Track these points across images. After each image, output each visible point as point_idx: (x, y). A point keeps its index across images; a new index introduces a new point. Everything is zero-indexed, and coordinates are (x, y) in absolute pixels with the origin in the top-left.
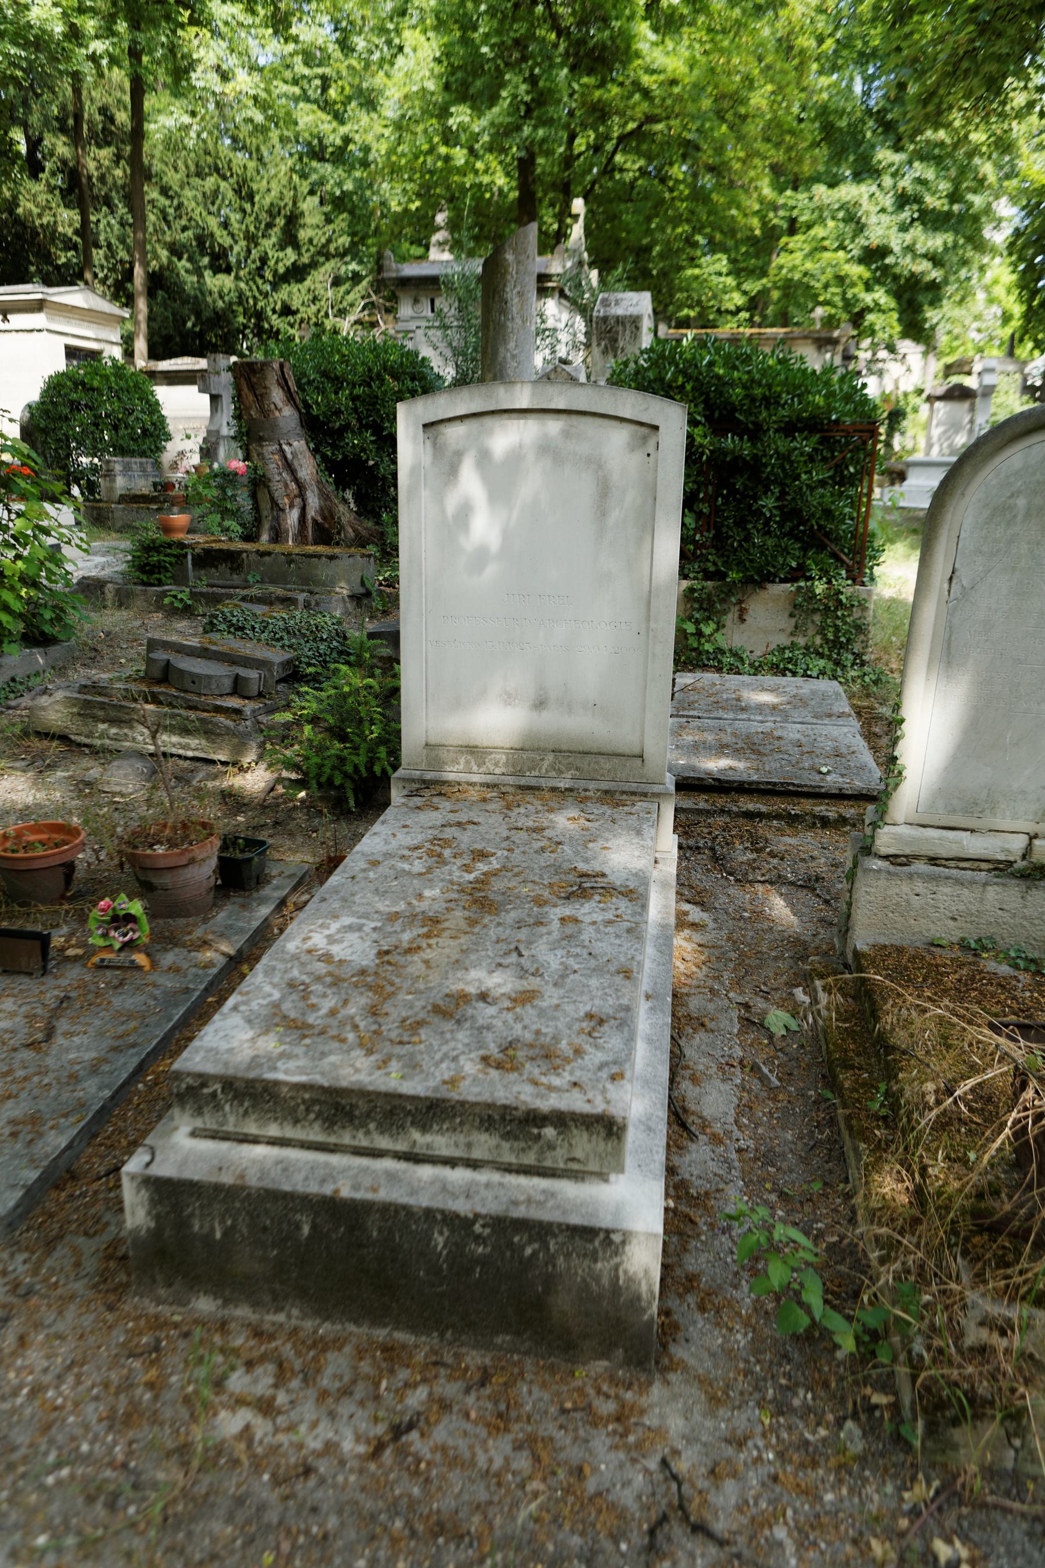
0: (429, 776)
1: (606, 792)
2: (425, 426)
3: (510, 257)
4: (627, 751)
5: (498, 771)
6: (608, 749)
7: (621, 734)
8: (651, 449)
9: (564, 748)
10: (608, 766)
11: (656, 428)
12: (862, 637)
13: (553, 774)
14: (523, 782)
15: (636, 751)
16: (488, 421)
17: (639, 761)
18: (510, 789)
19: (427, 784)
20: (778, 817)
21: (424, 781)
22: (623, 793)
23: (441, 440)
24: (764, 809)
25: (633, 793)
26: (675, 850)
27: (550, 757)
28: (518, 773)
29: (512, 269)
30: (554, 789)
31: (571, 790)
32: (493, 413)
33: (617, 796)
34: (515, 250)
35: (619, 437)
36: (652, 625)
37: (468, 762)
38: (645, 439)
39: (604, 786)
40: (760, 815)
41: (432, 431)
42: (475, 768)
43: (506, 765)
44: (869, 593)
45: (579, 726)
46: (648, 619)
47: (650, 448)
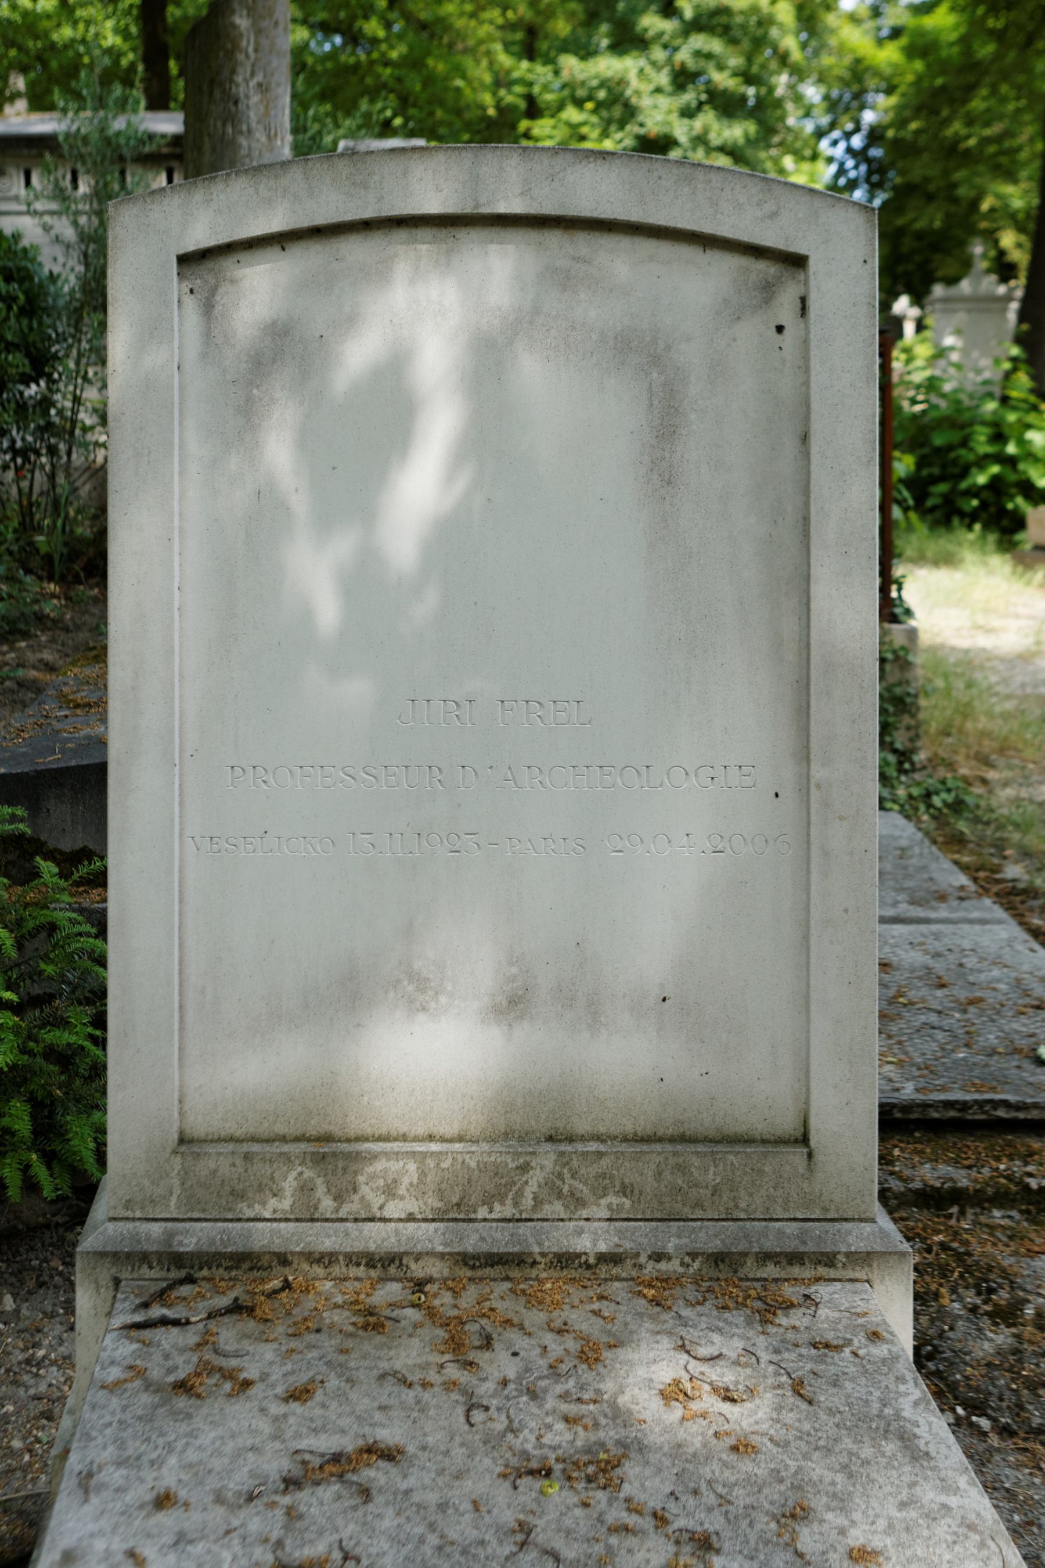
0: (193, 1238)
1: (718, 1259)
2: (185, 260)
3: (242, 21)
4: (759, 1127)
5: (394, 1209)
6: (705, 1122)
7: (753, 1089)
8: (785, 310)
9: (582, 1126)
10: (712, 1177)
11: (797, 262)
12: (907, 720)
13: (557, 1208)
14: (472, 1240)
15: (787, 1124)
16: (355, 250)
17: (796, 1157)
18: (435, 1269)
19: (185, 1268)
20: (1001, 1199)
21: (178, 1259)
22: (766, 1257)
23: (224, 296)
24: (963, 1179)
25: (795, 1258)
26: (951, 1436)
27: (546, 1159)
28: (455, 1212)
29: (247, 43)
30: (564, 1260)
31: (612, 1258)
32: (366, 226)
33: (750, 1268)
34: (251, 11)
35: (702, 284)
36: (818, 772)
37: (305, 1188)
38: (768, 290)
39: (710, 1237)
40: (957, 1197)
41: (204, 274)
42: (327, 1204)
43: (419, 1188)
44: (913, 634)
45: (627, 1066)
46: (804, 755)
47: (785, 310)
